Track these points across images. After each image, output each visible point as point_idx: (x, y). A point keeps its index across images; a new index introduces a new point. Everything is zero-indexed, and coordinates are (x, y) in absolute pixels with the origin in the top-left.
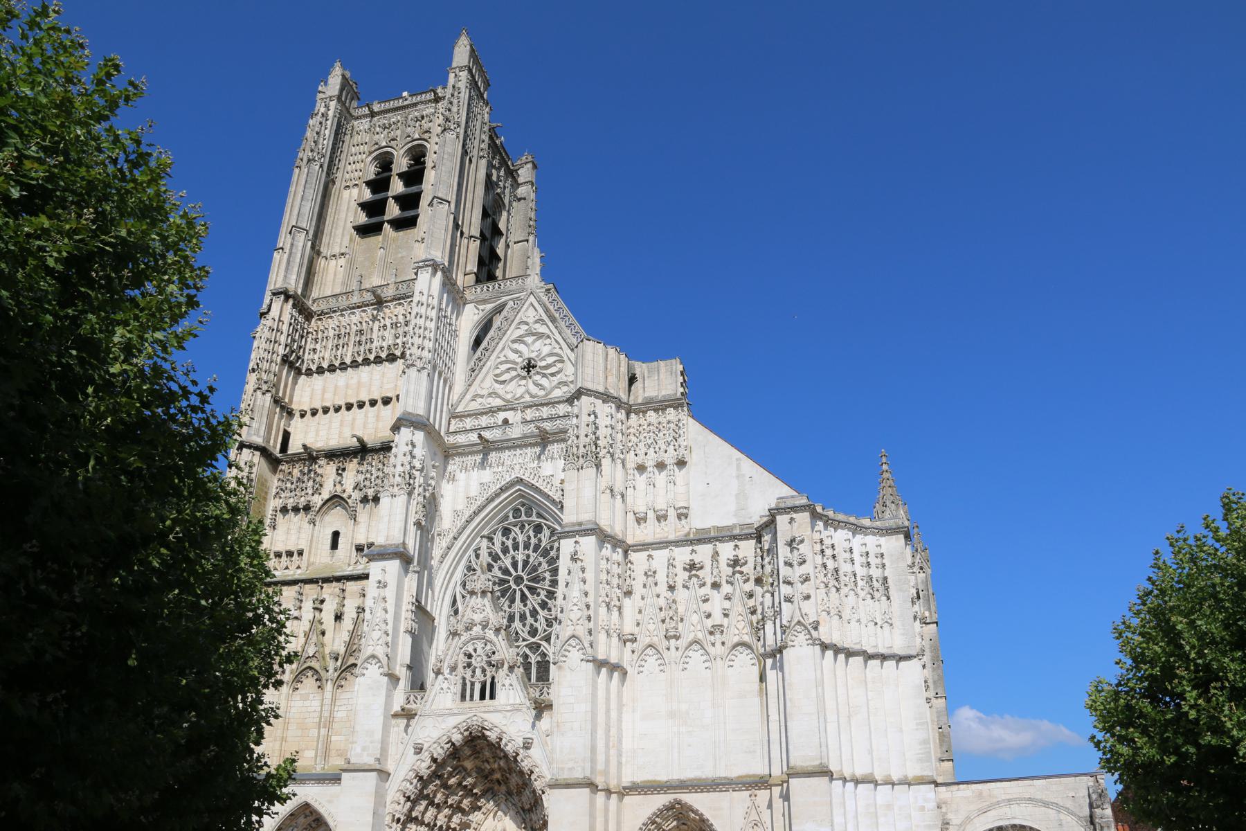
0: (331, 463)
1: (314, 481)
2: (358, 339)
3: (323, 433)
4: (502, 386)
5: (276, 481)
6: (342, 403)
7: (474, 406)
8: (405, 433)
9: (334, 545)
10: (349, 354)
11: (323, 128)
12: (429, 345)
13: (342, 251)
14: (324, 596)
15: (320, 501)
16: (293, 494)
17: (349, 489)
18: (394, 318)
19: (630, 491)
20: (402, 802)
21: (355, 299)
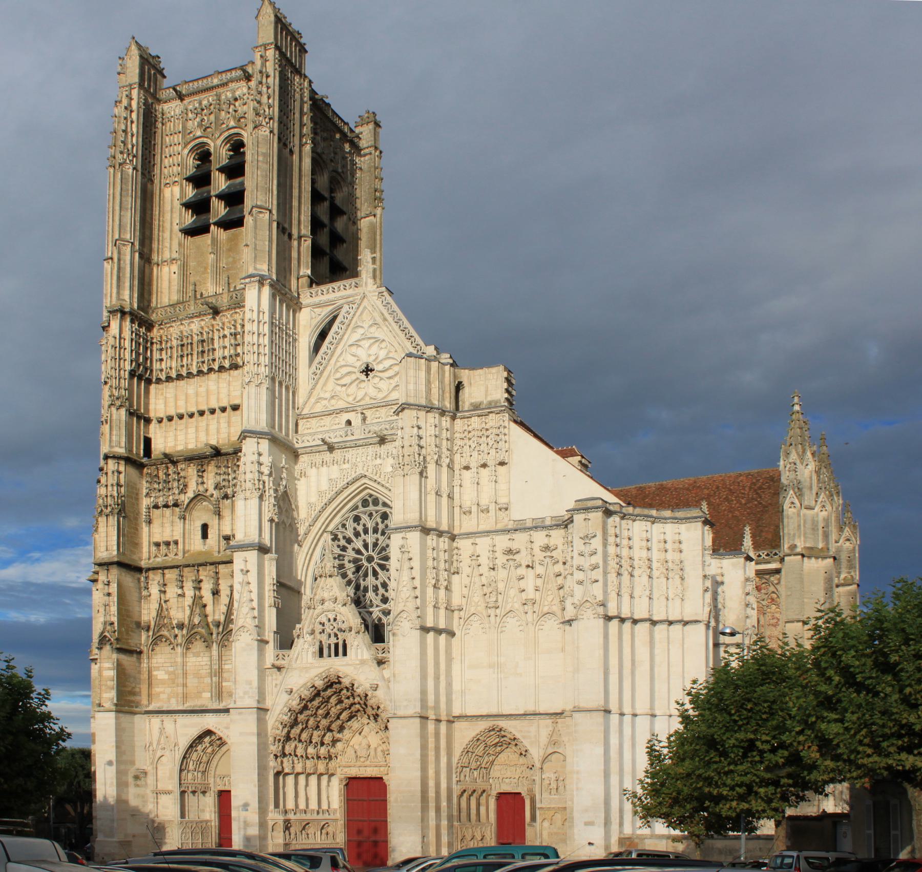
0: (192, 465)
2: (200, 349)
3: (181, 437)
5: (144, 483)
6: (194, 409)
9: (205, 535)
10: (195, 363)
14: (201, 578)
15: (186, 499)
16: (161, 493)
17: (211, 490)
18: (233, 327)
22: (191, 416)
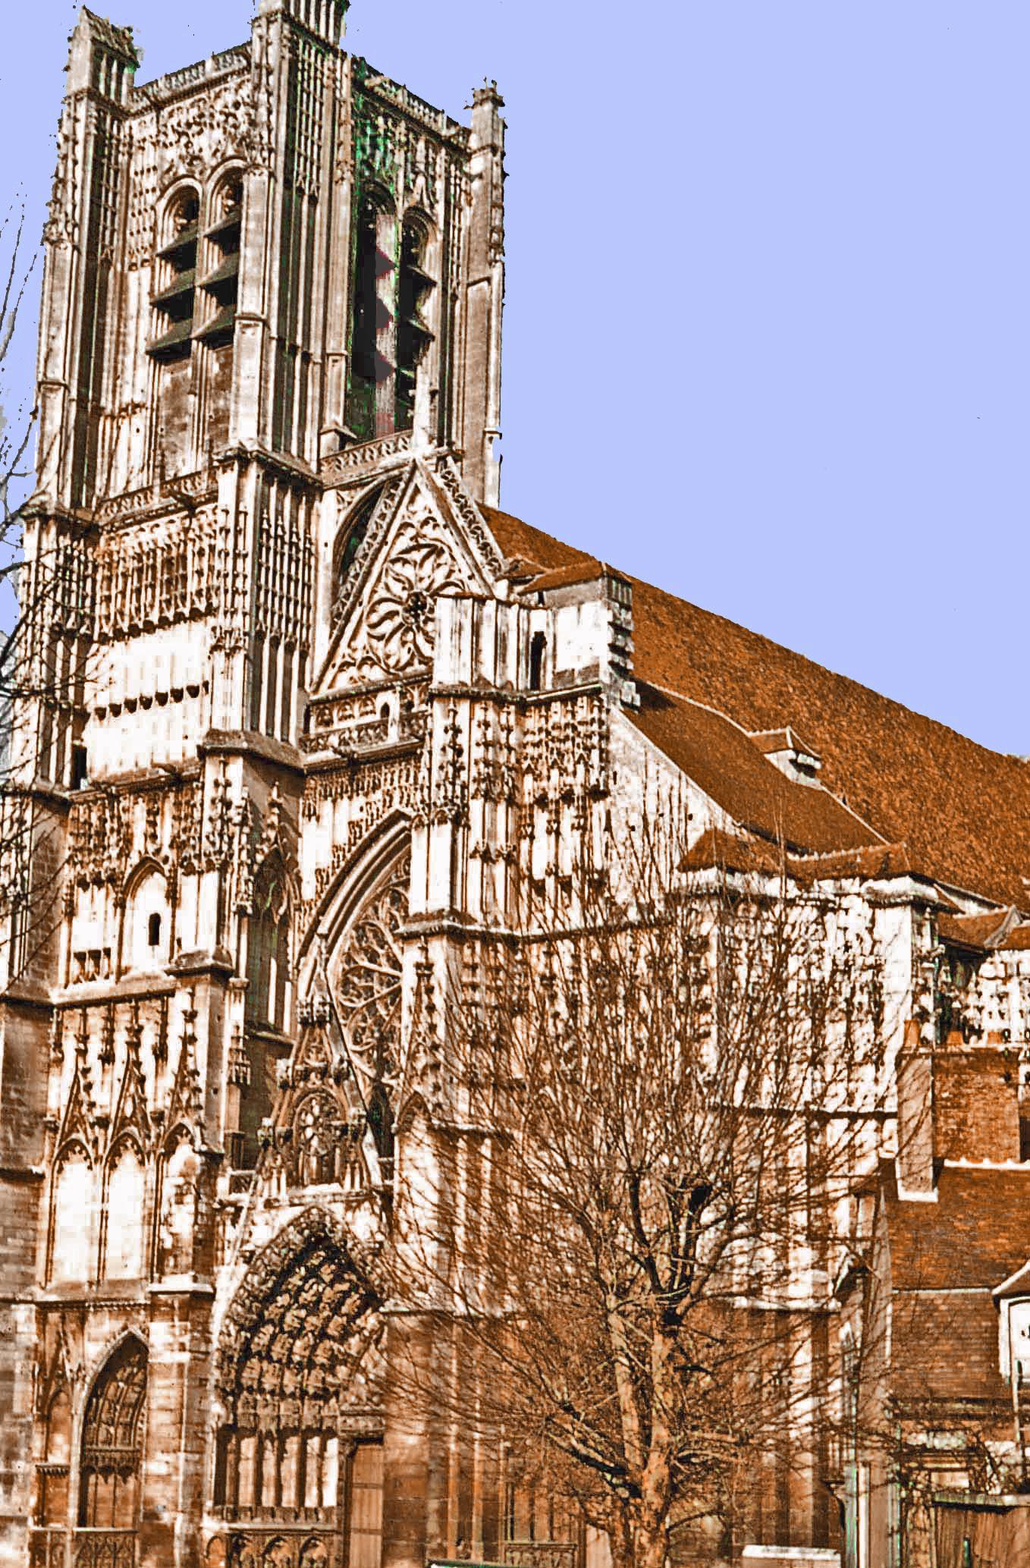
1: (119, 833)
2: (166, 576)
4: (382, 643)
7: (343, 683)
8: (212, 771)
9: (154, 939)
11: (70, 164)
12: (243, 603)
13: (137, 400)
17: (166, 851)
19: (525, 844)
20: (233, 1333)
21: (156, 502)
22: (147, 703)
